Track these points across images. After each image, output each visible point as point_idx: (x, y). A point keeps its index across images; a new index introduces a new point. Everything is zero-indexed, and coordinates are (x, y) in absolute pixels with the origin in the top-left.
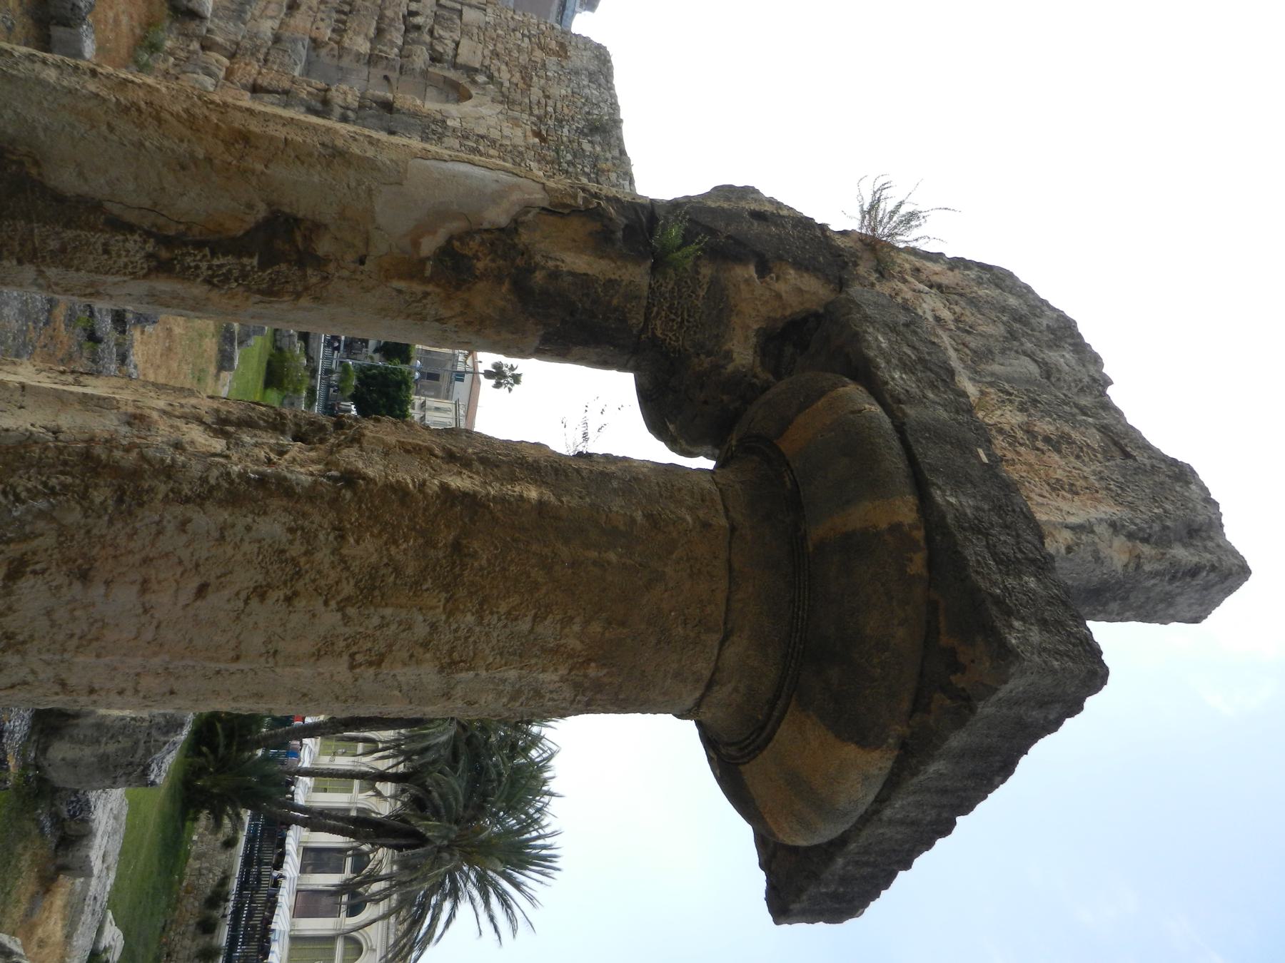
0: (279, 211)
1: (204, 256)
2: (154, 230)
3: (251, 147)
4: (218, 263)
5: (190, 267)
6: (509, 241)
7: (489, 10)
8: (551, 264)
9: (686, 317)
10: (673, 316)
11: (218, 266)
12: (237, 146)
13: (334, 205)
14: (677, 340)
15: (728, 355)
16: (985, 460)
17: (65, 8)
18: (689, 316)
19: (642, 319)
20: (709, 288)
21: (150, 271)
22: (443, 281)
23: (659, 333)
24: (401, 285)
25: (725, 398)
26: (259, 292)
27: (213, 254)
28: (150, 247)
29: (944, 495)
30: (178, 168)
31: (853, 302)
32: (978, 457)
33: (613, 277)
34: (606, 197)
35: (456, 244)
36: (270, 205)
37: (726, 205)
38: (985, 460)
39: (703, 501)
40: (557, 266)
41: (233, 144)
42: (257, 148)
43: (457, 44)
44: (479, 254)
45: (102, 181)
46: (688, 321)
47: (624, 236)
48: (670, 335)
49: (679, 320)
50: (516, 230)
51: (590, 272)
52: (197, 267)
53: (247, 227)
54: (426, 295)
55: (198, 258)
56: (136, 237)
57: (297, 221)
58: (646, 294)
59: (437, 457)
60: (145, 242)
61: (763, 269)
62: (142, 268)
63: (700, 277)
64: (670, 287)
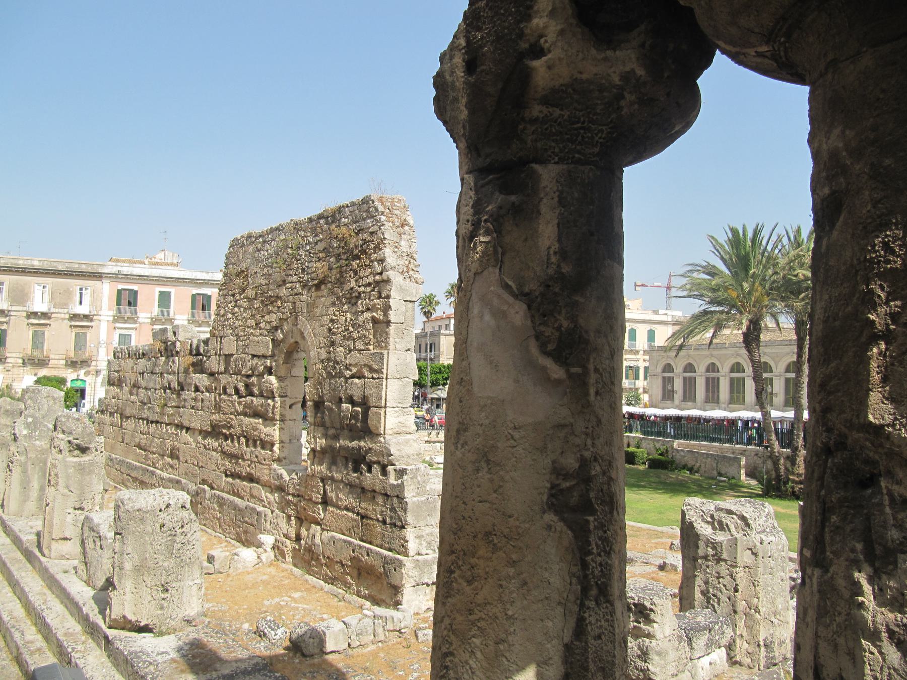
0: (547, 503)
1: (593, 560)
2: (578, 602)
3: (494, 530)
4: (595, 548)
5: (602, 571)
6: (539, 299)
7: (222, 333)
8: (554, 259)
9: (579, 125)
10: (580, 138)
11: (597, 549)
12: (496, 541)
13: (535, 457)
14: (602, 131)
15: (626, 77)
17: (313, 643)
18: (578, 122)
19: (589, 167)
20: (552, 106)
21: (608, 601)
22: (584, 356)
23: (596, 150)
24: (592, 391)
25: (666, 75)
26: (611, 513)
27: (590, 553)
28: (592, 604)
30: (525, 587)
33: (556, 199)
34: (474, 215)
35: (550, 347)
36: (544, 512)
37: (464, 101)
40: (555, 253)
41: (494, 545)
42: (494, 525)
43: (254, 356)
45: (549, 646)
46: (583, 123)
47: (513, 194)
48: (597, 138)
49: (582, 131)
50: (527, 295)
51: (556, 221)
52: (601, 565)
53: (565, 528)
54: (596, 370)
55: (594, 565)
56: (586, 615)
57: (553, 487)
58: (565, 167)
60: (589, 608)
61: (537, 52)
62: (607, 607)
63: (541, 115)
64: (553, 144)
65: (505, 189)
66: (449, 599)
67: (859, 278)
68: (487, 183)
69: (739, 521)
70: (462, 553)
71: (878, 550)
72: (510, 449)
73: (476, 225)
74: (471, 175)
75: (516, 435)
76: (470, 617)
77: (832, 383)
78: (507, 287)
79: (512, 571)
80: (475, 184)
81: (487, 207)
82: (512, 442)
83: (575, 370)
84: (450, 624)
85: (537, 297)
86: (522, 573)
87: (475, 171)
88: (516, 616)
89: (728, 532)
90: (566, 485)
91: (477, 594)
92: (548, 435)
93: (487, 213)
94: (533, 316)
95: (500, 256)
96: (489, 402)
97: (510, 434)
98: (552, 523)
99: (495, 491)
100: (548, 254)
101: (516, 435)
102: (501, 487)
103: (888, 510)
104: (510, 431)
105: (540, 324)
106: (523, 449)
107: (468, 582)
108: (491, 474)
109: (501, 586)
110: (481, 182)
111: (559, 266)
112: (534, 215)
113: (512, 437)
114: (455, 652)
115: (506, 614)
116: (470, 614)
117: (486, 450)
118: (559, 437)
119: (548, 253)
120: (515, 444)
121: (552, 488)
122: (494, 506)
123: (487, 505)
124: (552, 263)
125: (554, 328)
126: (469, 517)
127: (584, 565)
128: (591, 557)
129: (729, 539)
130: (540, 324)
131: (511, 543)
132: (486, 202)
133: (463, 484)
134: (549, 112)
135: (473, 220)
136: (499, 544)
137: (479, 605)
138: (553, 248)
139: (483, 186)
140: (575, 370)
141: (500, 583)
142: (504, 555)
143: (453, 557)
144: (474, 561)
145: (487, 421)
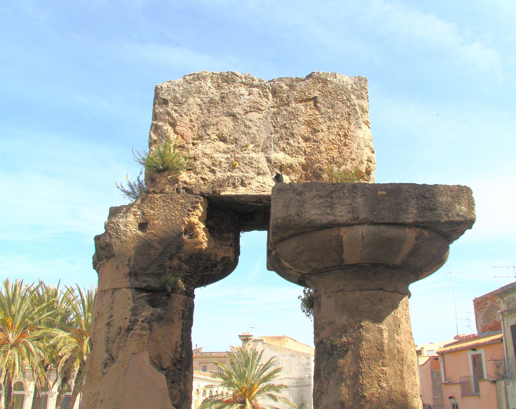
16: (385, 193)
29: (409, 218)
31: (286, 217)
32: (383, 195)
33: (181, 315)
34: (132, 316)
38: (385, 193)
39: (368, 299)
40: (180, 346)
44: (179, 388)
46: (191, 273)
48: (194, 282)
49: (189, 278)
51: (181, 327)
65: (153, 304)
68: (141, 298)
73: (134, 322)
74: (129, 290)
80: (133, 296)
81: (141, 313)
87: (132, 288)
93: (143, 316)
110: (137, 296)
111: (181, 353)
112: (170, 322)
124: (178, 352)
125: (178, 390)
130: (171, 387)
132: (141, 309)
134: (181, 265)
135: (130, 319)
138: (179, 342)
139: (138, 299)
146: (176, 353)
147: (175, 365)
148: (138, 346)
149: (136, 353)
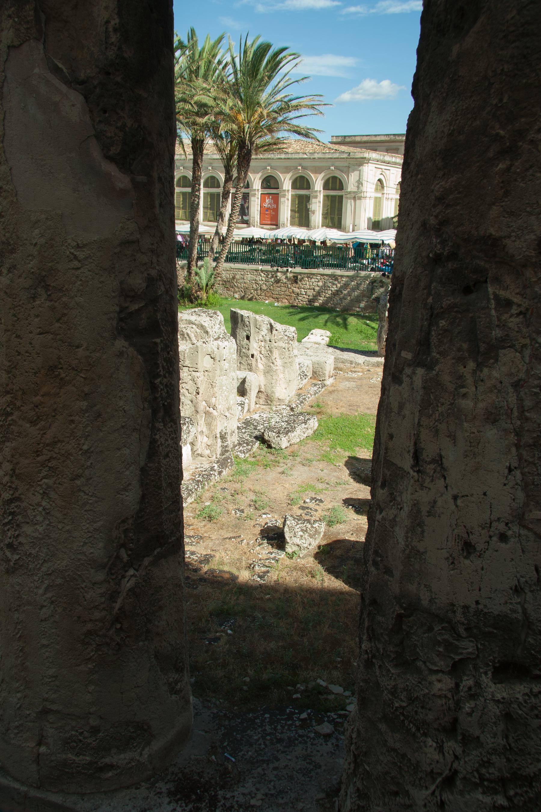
2: (150, 425)
3: (60, 363)
5: (168, 392)
6: (98, 90)
8: (114, 38)
11: (163, 371)
12: (63, 375)
13: (101, 280)
24: (157, 203)
27: (158, 376)
28: (160, 425)
35: (115, 150)
36: (115, 339)
40: (115, 30)
41: (62, 379)
42: (59, 358)
44: (119, 125)
45: (127, 473)
50: (82, 83)
52: (166, 385)
54: (160, 179)
56: (157, 437)
59: (511, 165)
60: (159, 430)
62: (171, 426)
66: (8, 444)
67: (493, 91)
69: (198, 331)
70: (20, 393)
71: (483, 347)
72: (73, 271)
75: (81, 255)
76: (39, 459)
77: (451, 197)
78: (56, 70)
79: (84, 404)
82: (76, 263)
83: (141, 178)
84: (11, 470)
85: (95, 87)
86: (95, 405)
88: (92, 449)
89: (189, 341)
90: (135, 307)
91: (44, 433)
92: (115, 253)
94: (91, 111)
95: (43, 25)
96: (43, 216)
97: (72, 254)
98: (125, 349)
99: (58, 321)
100: (107, 31)
101: (81, 255)
102: (65, 315)
103: (493, 312)
104: (72, 251)
105: (100, 122)
106: (89, 271)
107: (31, 422)
108: (51, 301)
109: (72, 421)
113: (76, 257)
114: (23, 497)
115: (81, 449)
116: (38, 456)
117: (44, 273)
118: (126, 255)
119: (107, 28)
120: (79, 265)
121: (121, 312)
122: (58, 337)
123: (51, 336)
125: (117, 128)
126: (27, 352)
127: (154, 388)
128: (159, 380)
129: (191, 348)
130: (100, 122)
131: (81, 375)
133: (14, 315)
136: (68, 378)
137: (48, 445)
138: (113, 23)
140: (141, 178)
141: (72, 418)
142: (73, 388)
143: (8, 398)
144: (37, 399)
145: (43, 241)
146: (106, 48)
147: (108, 74)
148: (16, 29)
149: (14, 47)
